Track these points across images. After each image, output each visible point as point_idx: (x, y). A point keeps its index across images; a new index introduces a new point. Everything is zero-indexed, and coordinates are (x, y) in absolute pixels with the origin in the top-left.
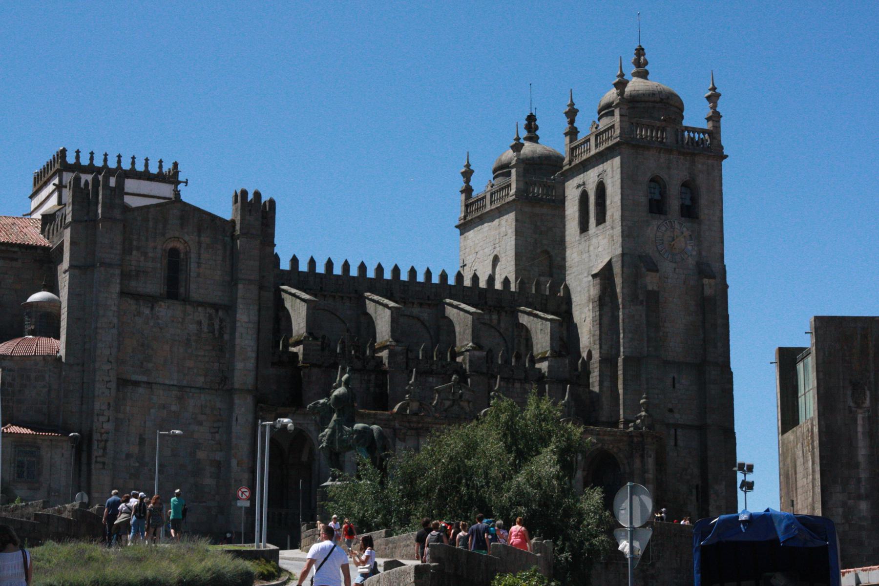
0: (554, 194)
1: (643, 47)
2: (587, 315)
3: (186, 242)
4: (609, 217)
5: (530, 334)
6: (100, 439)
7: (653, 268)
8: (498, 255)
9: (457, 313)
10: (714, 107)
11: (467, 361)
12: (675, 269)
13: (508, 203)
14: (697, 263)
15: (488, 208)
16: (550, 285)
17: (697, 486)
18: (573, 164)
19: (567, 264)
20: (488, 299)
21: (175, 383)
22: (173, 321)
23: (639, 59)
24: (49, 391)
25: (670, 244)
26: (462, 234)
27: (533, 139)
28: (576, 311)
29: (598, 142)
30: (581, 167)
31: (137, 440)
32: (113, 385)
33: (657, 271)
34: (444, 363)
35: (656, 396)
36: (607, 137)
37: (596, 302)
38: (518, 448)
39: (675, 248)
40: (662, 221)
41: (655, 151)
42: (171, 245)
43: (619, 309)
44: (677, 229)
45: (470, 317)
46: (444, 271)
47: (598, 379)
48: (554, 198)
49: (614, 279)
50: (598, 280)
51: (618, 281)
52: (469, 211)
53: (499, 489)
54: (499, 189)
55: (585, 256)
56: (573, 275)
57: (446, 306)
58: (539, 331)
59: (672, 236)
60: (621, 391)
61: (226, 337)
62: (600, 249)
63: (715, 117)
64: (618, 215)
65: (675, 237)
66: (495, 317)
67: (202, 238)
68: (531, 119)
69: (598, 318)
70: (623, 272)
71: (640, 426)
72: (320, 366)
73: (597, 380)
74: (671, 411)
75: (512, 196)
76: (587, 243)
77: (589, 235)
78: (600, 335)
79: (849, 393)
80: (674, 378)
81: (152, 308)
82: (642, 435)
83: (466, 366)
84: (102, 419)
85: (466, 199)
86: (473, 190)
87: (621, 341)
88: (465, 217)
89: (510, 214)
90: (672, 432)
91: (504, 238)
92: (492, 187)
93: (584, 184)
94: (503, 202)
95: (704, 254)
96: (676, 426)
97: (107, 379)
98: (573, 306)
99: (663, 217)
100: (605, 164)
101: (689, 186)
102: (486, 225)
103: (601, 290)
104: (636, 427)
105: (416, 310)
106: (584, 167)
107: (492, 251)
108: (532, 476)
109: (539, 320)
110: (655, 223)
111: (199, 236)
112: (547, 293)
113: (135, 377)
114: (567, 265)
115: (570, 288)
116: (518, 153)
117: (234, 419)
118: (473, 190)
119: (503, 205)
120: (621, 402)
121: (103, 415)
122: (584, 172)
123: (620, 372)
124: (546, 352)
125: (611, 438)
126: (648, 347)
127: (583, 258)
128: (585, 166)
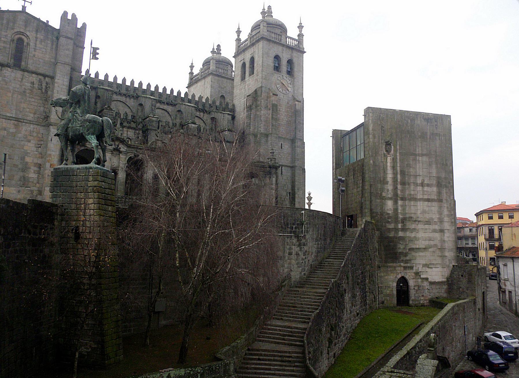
3: (28, 36)
15: (200, 78)
21: (14, 116)
22: (15, 80)
61: (49, 93)
67: (38, 36)
68: (219, 46)
79: (384, 146)
96: (282, 166)
101: (290, 62)
105: (165, 107)
110: (276, 75)
111: (37, 34)
117: (50, 140)
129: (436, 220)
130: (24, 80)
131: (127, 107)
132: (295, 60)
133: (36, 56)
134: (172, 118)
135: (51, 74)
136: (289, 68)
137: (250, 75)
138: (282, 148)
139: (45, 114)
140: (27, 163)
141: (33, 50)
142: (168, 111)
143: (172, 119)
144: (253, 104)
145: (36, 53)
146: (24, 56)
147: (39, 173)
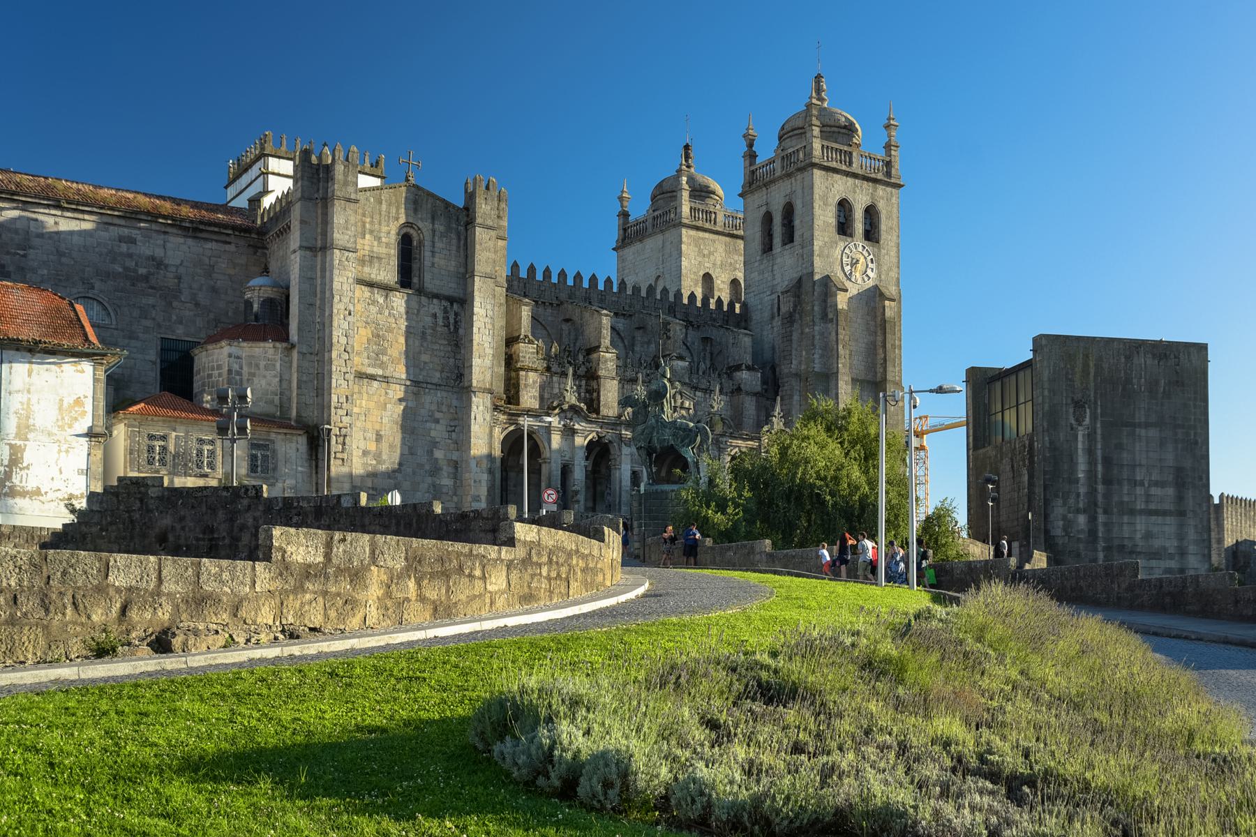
3: (419, 229)
6: (338, 433)
18: (754, 186)
24: (281, 381)
31: (374, 436)
32: (350, 377)
42: (405, 230)
61: (461, 331)
72: (536, 370)
81: (387, 297)
84: (340, 412)
97: (344, 370)
99: (849, 239)
111: (433, 224)
113: (371, 371)
121: (341, 408)
129: (1171, 551)
130: (422, 312)
131: (540, 326)
132: (881, 205)
133: (436, 265)
134: (626, 343)
135: (461, 296)
137: (784, 244)
139: (457, 372)
140: (436, 459)
141: (430, 254)
142: (617, 329)
143: (625, 346)
144: (794, 311)
145: (436, 260)
146: (415, 266)
147: (455, 478)
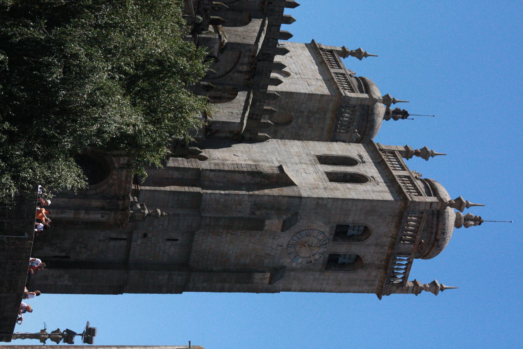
0: (341, 131)
1: (482, 223)
2: (240, 158)
4: (335, 185)
5: (225, 102)
7: (285, 227)
8: (290, 76)
9: (255, 30)
10: (425, 288)
11: (209, 36)
12: (281, 246)
13: (338, 89)
14: (285, 267)
15: (332, 71)
16: (270, 123)
17: (69, 257)
18: (380, 152)
19: (287, 141)
20: (263, 62)
23: (471, 220)
25: (306, 243)
26: (307, 45)
27: (388, 116)
28: (244, 147)
29: (404, 179)
30: (379, 161)
33: (283, 230)
34: (209, 12)
35: (161, 223)
36: (409, 187)
37: (256, 169)
38: (139, 77)
39: (301, 247)
40: (328, 236)
41: (394, 233)
43: (248, 191)
44: (319, 250)
45: (253, 42)
46: (294, 20)
47: (181, 166)
48: (338, 130)
49: (277, 188)
50: (277, 171)
51: (275, 192)
52: (327, 53)
53: (92, 42)
54: (349, 82)
55: (296, 159)
56: (277, 146)
57: (262, 19)
58: (230, 110)
59: (313, 245)
60: (168, 188)
62: (304, 174)
63: (416, 289)
64: (338, 194)
65: (311, 248)
66: (245, 68)
68: (404, 114)
69: (241, 169)
70: (284, 197)
71: (134, 208)
73: (179, 165)
74: (145, 236)
75: (345, 93)
76: (309, 162)
77: (316, 164)
78: (224, 171)
80: (177, 240)
82: (125, 209)
83: (204, 34)
85: (337, 51)
86: (344, 58)
87: (217, 192)
88: (322, 49)
89: (327, 90)
90: (124, 236)
91: (306, 83)
92: (350, 75)
93: (364, 162)
94: (338, 85)
95: (293, 273)
96: (129, 240)
98: (248, 145)
99: (331, 237)
100: (385, 184)
102: (317, 67)
103: (267, 173)
104: (134, 203)
106: (379, 163)
107: (293, 71)
108: (106, 94)
109: (242, 112)
110: (327, 229)
112: (262, 121)
114: (286, 140)
115: (265, 142)
116: (382, 101)
118: (344, 58)
119: (336, 84)
120: (157, 188)
122: (374, 162)
123: (187, 189)
124: (210, 116)
125: (124, 178)
126: (210, 217)
127: (294, 157)
128: (380, 164)
132: (362, 274)
136: (346, 261)
137: (328, 174)
138: (168, 240)
